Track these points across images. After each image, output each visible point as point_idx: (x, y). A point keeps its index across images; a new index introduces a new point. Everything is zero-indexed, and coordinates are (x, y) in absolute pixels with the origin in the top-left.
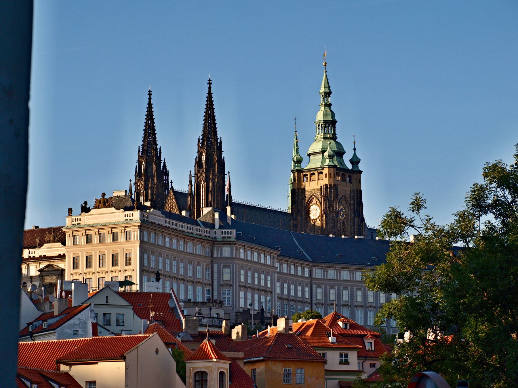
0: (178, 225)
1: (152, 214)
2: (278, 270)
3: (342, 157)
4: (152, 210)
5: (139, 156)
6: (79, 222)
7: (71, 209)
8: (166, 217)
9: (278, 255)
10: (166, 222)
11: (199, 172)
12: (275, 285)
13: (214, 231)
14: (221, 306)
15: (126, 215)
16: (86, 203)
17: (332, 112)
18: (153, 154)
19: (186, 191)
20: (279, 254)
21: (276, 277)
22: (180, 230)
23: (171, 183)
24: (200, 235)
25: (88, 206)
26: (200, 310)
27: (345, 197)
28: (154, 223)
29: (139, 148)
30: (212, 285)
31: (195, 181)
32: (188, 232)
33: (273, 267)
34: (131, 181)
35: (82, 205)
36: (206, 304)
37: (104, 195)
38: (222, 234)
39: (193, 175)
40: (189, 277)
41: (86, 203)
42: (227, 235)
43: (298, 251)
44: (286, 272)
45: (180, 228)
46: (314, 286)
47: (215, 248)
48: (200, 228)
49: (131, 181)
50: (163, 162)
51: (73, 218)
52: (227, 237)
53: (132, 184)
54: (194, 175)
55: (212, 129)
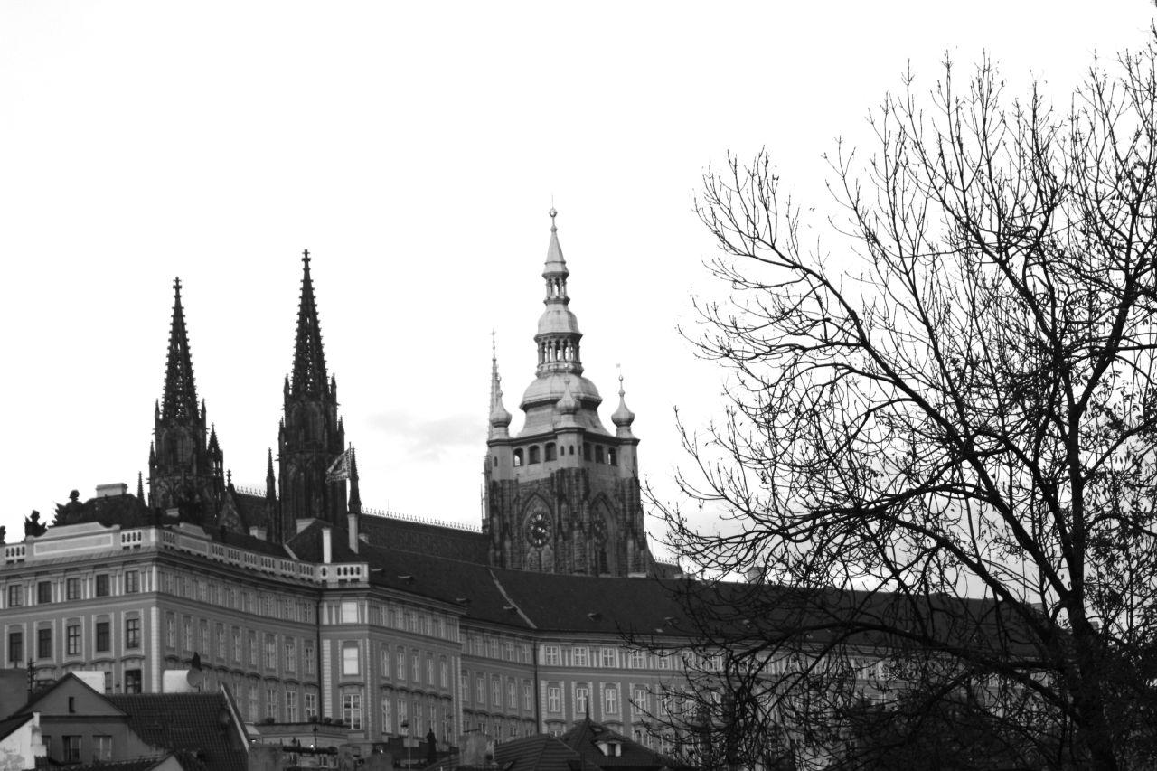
0: (242, 557)
1: (182, 534)
3: (596, 410)
6: (21, 557)
13: (321, 567)
16: (36, 515)
18: (188, 413)
19: (263, 493)
20: (464, 614)
21: (459, 666)
23: (229, 476)
24: (291, 577)
25: (40, 522)
27: (605, 497)
28: (189, 552)
30: (319, 686)
33: (453, 643)
34: (140, 474)
35: (27, 520)
37: (75, 494)
39: (275, 456)
40: (268, 669)
41: (36, 515)
43: (505, 608)
46: (543, 684)
47: (325, 605)
50: (209, 432)
51: (6, 548)
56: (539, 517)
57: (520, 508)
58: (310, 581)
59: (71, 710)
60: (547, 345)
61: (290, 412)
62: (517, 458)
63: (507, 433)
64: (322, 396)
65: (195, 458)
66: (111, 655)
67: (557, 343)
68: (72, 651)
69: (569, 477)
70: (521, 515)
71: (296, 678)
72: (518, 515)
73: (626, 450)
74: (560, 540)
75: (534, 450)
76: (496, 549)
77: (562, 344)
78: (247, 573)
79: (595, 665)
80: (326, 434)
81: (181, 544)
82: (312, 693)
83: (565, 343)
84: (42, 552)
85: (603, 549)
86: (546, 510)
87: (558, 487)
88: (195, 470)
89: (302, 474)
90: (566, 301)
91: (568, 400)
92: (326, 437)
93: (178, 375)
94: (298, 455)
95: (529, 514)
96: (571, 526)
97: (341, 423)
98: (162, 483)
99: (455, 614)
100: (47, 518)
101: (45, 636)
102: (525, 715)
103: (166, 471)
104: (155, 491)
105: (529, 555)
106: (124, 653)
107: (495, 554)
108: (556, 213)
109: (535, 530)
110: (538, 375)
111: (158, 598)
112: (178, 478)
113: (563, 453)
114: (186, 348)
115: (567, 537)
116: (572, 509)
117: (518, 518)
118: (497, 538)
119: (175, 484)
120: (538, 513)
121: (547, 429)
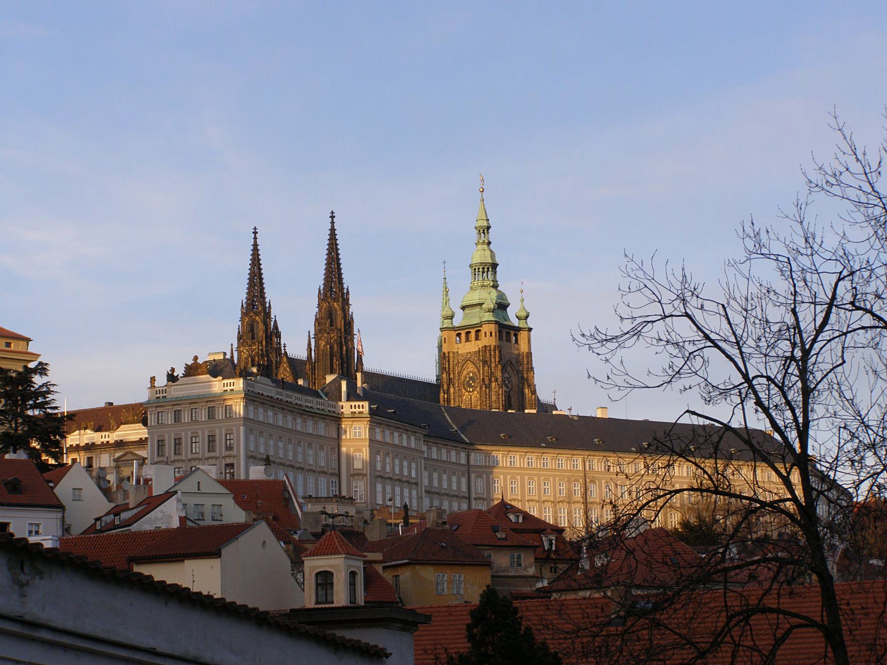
0: (294, 397)
2: (426, 456)
3: (506, 310)
4: (258, 377)
5: (242, 312)
7: (154, 377)
8: (277, 387)
9: (425, 435)
10: (278, 393)
11: (320, 331)
12: (421, 476)
14: (352, 502)
15: (226, 384)
16: (173, 370)
17: (491, 251)
18: (260, 309)
21: (423, 465)
22: (297, 404)
23: (285, 347)
24: (323, 410)
25: (175, 374)
26: (324, 508)
27: (511, 363)
28: (262, 394)
29: (242, 303)
30: (339, 476)
31: (315, 344)
32: (307, 406)
34: (232, 345)
36: (332, 500)
37: (196, 358)
38: (351, 408)
39: (312, 336)
41: (173, 370)
42: (357, 410)
43: (451, 430)
44: (436, 458)
45: (297, 401)
46: (473, 476)
48: (323, 401)
49: (232, 345)
50: (273, 320)
52: (357, 412)
53: (234, 349)
54: (314, 336)
55: (337, 275)
56: (471, 375)
57: (460, 369)
58: (334, 412)
59: (199, 490)
60: (477, 270)
61: (321, 309)
62: (458, 338)
63: (452, 324)
64: (341, 299)
65: (264, 336)
66: (217, 454)
67: (483, 268)
68: (194, 452)
69: (490, 350)
70: (460, 373)
71: (325, 470)
72: (458, 373)
73: (523, 335)
74: (484, 389)
75: (468, 333)
76: (444, 394)
77: (486, 270)
78: (296, 407)
79: (505, 465)
80: (343, 323)
81: (258, 389)
82: (335, 479)
83: (488, 268)
84: (176, 391)
85: (509, 395)
86: (476, 370)
87: (483, 356)
88: (264, 343)
89: (328, 346)
90: (489, 243)
91: (490, 304)
92: (343, 325)
93: (255, 285)
94: (326, 335)
95: (465, 372)
96: (490, 380)
97: (352, 316)
98: (245, 351)
99: (420, 433)
100: (180, 372)
101: (178, 442)
102: (462, 494)
103: (247, 343)
104: (241, 355)
105: (464, 397)
106: (224, 453)
107: (444, 396)
108: (483, 190)
109: (468, 381)
110: (471, 288)
111: (244, 421)
112: (255, 347)
113: (486, 336)
114: (260, 269)
115: (489, 386)
116: (491, 370)
117: (459, 375)
118: (445, 387)
119: (253, 351)
120: (470, 372)
121: (476, 321)
